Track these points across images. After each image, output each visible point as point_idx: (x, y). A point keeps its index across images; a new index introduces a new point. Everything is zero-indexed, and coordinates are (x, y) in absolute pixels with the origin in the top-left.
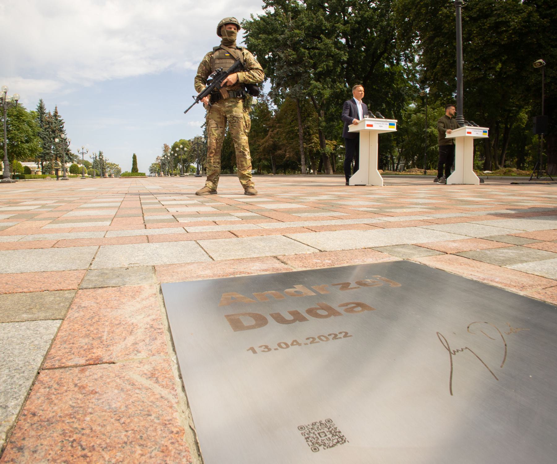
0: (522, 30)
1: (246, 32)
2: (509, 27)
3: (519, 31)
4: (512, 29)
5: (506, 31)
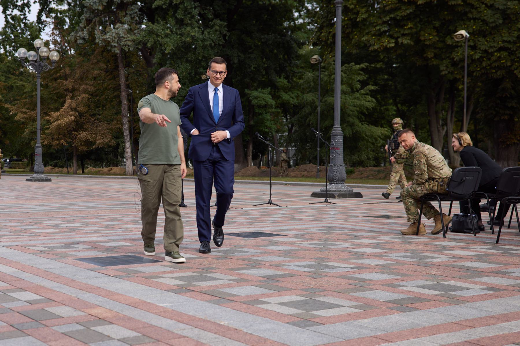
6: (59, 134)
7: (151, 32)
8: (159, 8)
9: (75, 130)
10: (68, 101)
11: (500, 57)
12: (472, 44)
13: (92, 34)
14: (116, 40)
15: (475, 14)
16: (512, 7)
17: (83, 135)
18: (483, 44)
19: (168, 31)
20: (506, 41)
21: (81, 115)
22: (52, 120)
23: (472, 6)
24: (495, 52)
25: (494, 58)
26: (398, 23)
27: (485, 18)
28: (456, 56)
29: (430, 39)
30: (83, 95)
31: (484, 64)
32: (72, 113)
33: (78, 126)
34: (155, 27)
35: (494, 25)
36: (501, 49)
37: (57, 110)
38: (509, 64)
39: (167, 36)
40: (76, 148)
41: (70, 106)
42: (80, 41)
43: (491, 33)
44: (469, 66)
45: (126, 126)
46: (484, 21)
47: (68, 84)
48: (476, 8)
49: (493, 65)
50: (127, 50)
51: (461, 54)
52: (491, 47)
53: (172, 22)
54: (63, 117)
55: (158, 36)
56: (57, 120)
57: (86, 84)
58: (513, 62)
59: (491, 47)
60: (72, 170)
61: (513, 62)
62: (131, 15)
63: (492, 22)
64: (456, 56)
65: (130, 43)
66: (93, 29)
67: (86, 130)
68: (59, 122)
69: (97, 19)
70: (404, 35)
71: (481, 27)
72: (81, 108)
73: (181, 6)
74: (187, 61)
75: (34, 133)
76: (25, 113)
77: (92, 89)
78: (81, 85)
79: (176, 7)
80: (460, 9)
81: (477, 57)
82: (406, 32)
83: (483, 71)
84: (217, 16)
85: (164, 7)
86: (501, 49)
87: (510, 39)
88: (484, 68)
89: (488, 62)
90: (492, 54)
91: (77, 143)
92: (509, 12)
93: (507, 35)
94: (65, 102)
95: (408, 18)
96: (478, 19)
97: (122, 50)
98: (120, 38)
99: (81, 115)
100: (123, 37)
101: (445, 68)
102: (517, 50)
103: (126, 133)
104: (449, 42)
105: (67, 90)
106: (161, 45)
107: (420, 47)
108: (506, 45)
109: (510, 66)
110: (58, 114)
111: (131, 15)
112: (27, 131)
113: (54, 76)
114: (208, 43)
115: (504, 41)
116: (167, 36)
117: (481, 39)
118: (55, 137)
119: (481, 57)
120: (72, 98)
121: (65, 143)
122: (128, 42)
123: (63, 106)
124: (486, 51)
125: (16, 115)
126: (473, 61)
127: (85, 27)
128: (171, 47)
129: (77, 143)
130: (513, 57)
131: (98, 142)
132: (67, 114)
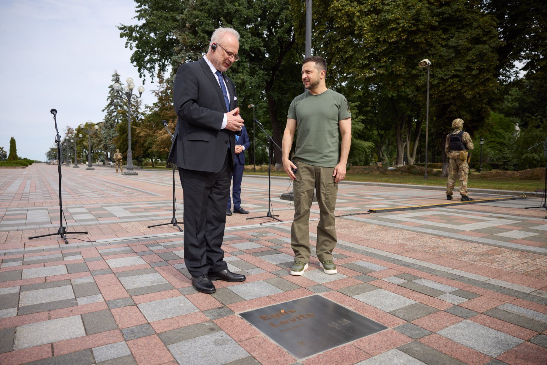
0: (411, 27)
1: (140, 6)
2: (399, 24)
3: (408, 28)
4: (401, 27)
5: (396, 29)
11: (452, 83)
12: (432, 73)
15: (433, 51)
16: (463, 43)
18: (440, 73)
20: (458, 70)
23: (431, 46)
24: (449, 79)
25: (448, 84)
26: (376, 58)
27: (442, 53)
28: (419, 82)
29: (400, 70)
31: (441, 89)
35: (448, 57)
36: (454, 76)
38: (459, 88)
43: (445, 65)
44: (430, 89)
46: (440, 56)
48: (434, 47)
49: (447, 89)
51: (424, 81)
52: (446, 75)
58: (463, 86)
59: (446, 75)
61: (463, 86)
63: (447, 56)
64: (419, 82)
70: (380, 67)
71: (438, 61)
80: (423, 46)
81: (435, 82)
82: (383, 64)
83: (440, 94)
86: (454, 76)
87: (460, 68)
88: (441, 91)
89: (444, 87)
90: (447, 80)
92: (460, 48)
93: (458, 65)
95: (384, 54)
96: (436, 54)
101: (411, 93)
102: (466, 77)
104: (414, 72)
107: (393, 76)
108: (458, 73)
109: (460, 90)
115: (456, 70)
117: (438, 70)
119: (438, 83)
124: (442, 79)
126: (432, 86)
130: (463, 83)
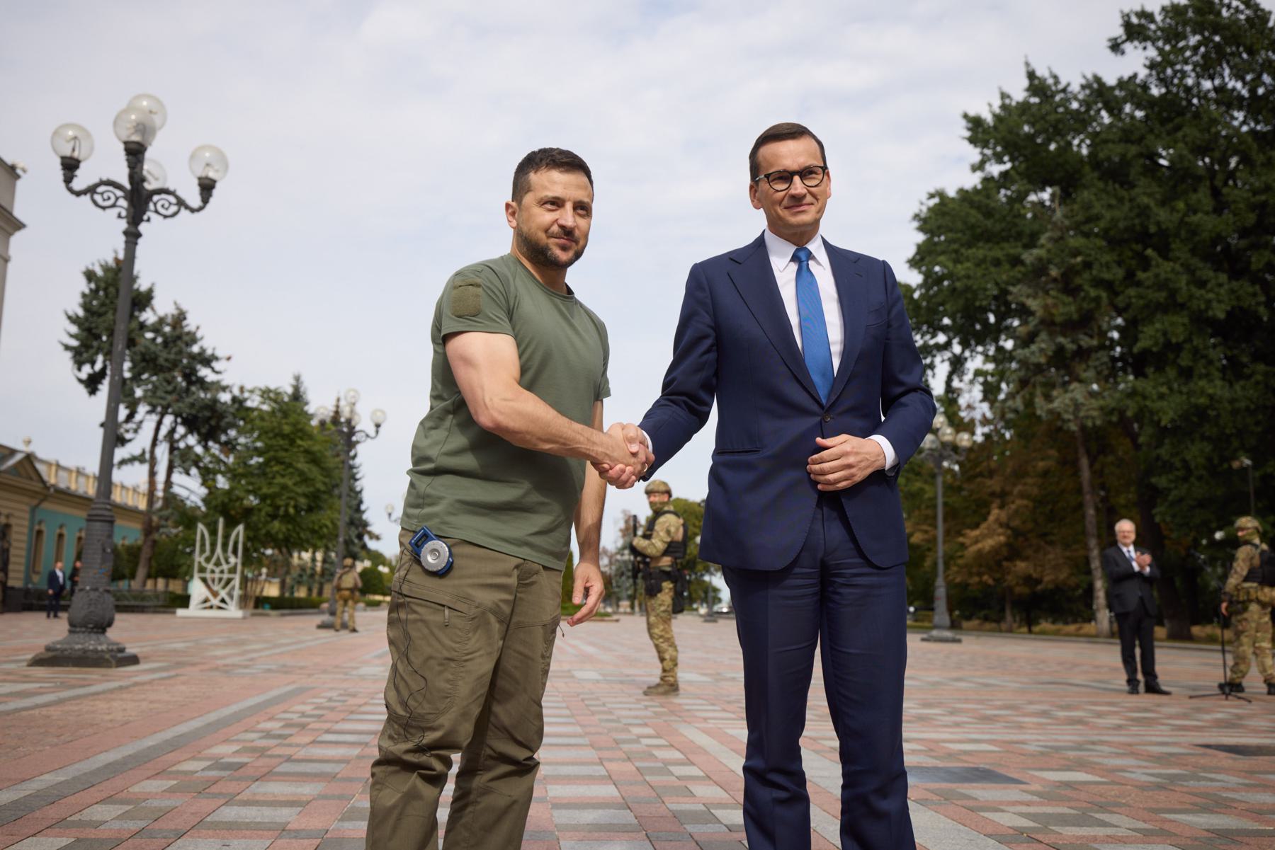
6: (981, 566)
7: (1133, 394)
8: (1145, 352)
9: (1008, 559)
10: (995, 513)
13: (1029, 404)
14: (1071, 410)
17: (1021, 566)
19: (1164, 389)
21: (1016, 533)
22: (966, 541)
30: (1019, 502)
32: (1000, 530)
33: (1012, 552)
34: (1141, 384)
37: (977, 526)
39: (1161, 397)
40: (1010, 589)
41: (997, 520)
42: (1010, 416)
45: (1095, 553)
47: (994, 484)
50: (1089, 423)
53: (1171, 373)
54: (986, 538)
55: (1145, 397)
56: (976, 542)
57: (1025, 484)
60: (1004, 626)
62: (1095, 367)
65: (1095, 413)
66: (1032, 395)
67: (1026, 559)
68: (980, 546)
69: (1040, 378)
72: (1016, 523)
73: (1187, 346)
74: (1203, 438)
75: (935, 564)
76: (926, 532)
77: (1035, 491)
78: (1014, 485)
79: (1178, 348)
84: (1257, 357)
85: (1155, 349)
91: (1010, 580)
94: (989, 513)
97: (1083, 428)
98: (1077, 406)
99: (1016, 533)
100: (1083, 404)
103: (1096, 564)
105: (993, 494)
106: (1152, 413)
110: (976, 533)
111: (1095, 367)
112: (928, 563)
113: (972, 473)
114: (1243, 405)
116: (1161, 397)
118: (974, 570)
120: (1001, 507)
121: (991, 582)
122: (1093, 414)
123: (985, 519)
125: (911, 535)
127: (1018, 392)
128: (1171, 414)
129: (1010, 580)
131: (1047, 579)
132: (991, 534)
